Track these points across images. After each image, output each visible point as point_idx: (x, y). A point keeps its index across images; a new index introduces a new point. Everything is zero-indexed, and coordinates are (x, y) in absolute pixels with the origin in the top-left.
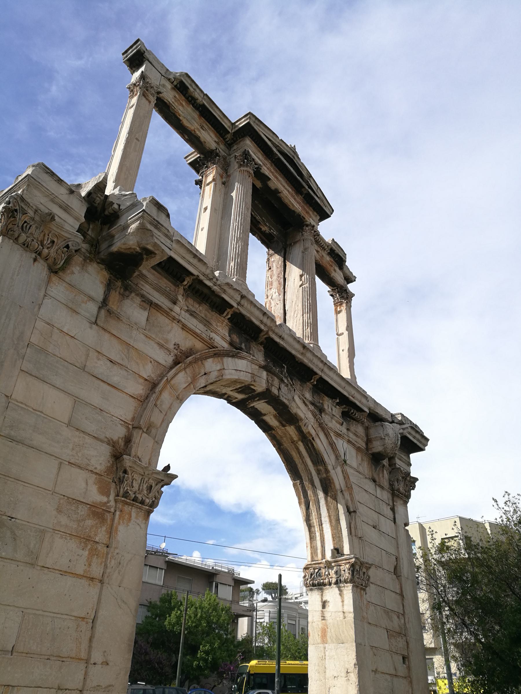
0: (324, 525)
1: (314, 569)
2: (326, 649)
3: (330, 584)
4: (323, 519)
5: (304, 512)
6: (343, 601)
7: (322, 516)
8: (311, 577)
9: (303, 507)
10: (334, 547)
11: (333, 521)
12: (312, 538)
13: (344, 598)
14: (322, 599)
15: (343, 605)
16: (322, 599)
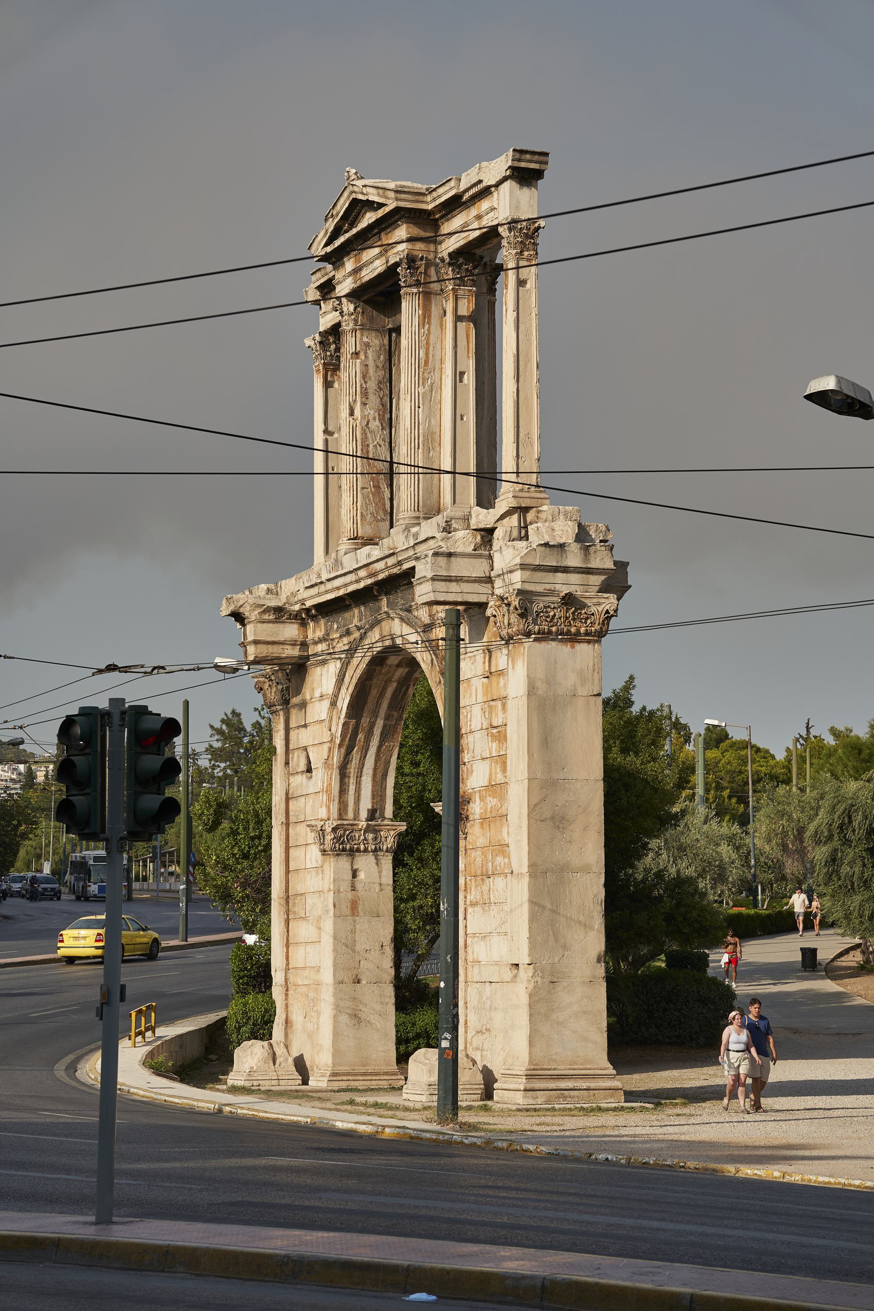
0: (363, 778)
1: (345, 831)
2: (357, 922)
3: (366, 850)
4: (365, 770)
5: (342, 757)
6: (380, 872)
7: (365, 767)
8: (340, 840)
9: (343, 750)
10: (373, 806)
11: (379, 776)
12: (343, 791)
13: (381, 868)
14: (352, 867)
15: (380, 876)
16: (352, 867)
